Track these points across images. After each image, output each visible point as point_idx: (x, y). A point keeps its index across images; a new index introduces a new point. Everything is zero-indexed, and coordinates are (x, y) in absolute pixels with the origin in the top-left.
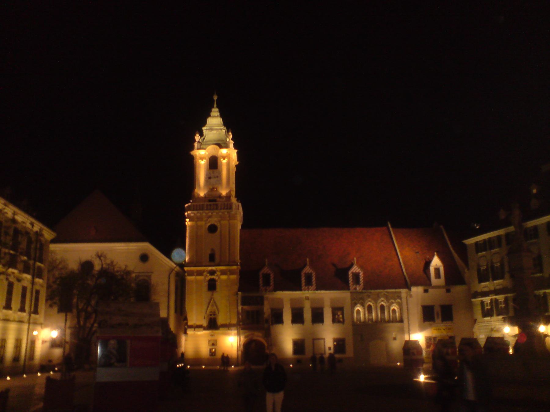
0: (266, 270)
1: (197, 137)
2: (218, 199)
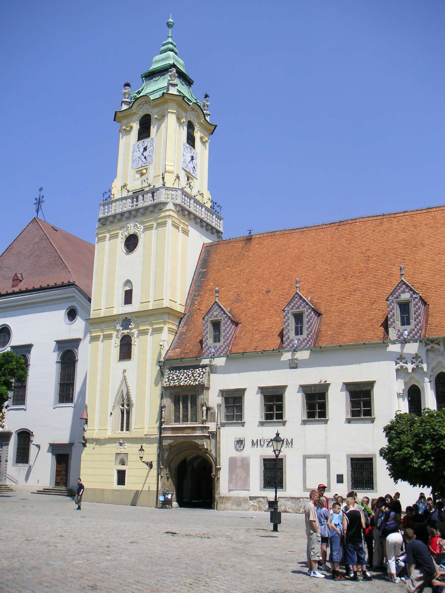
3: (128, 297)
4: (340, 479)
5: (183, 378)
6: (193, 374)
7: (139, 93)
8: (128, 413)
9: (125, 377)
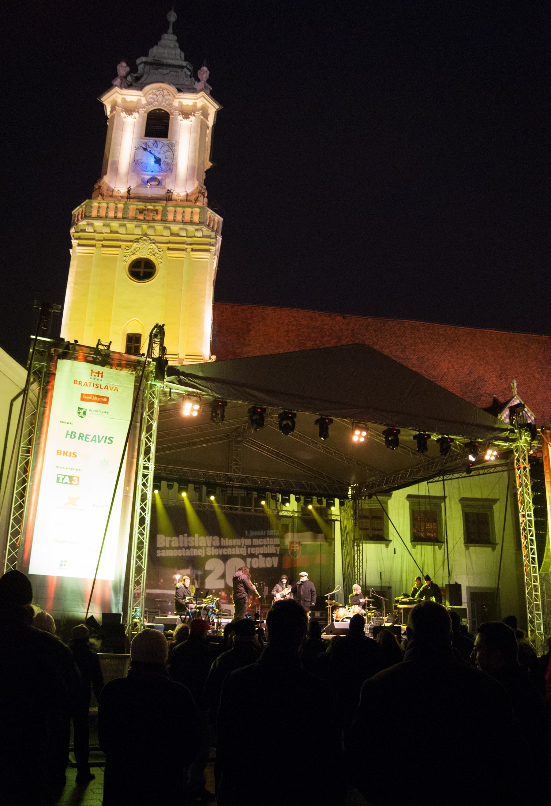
1: (123, 68)
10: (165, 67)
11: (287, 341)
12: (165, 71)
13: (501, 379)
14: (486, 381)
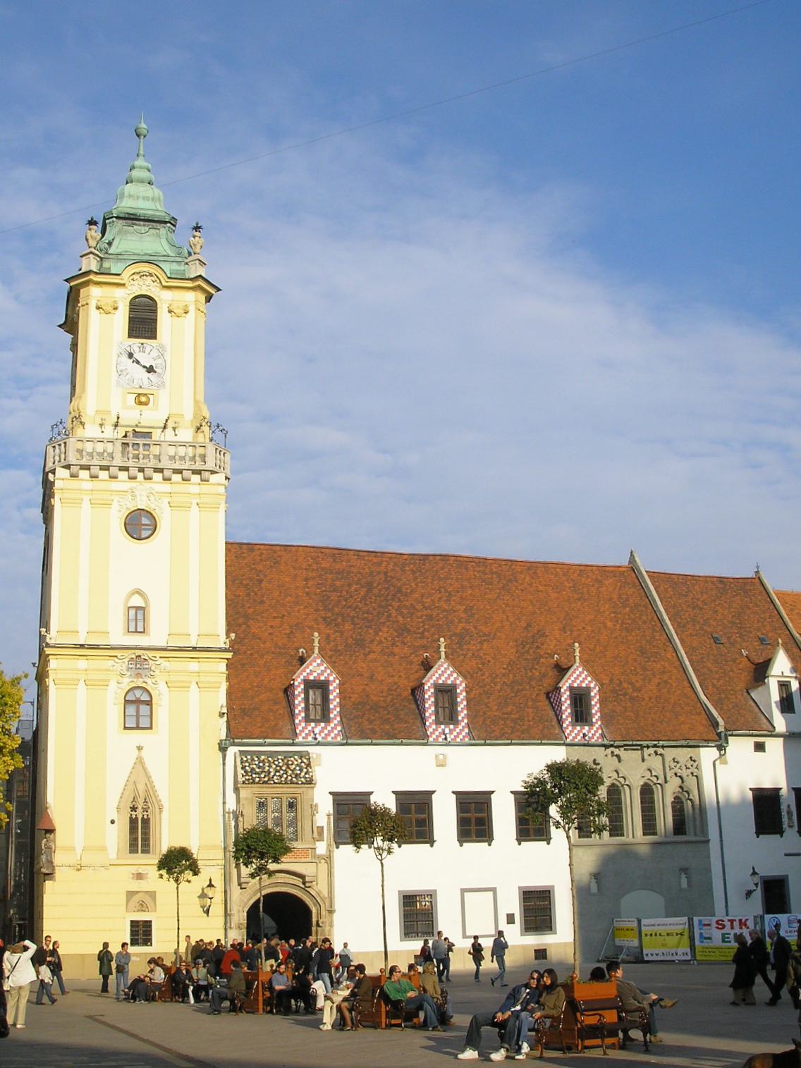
0: (316, 668)
2: (157, 435)
3: (138, 617)
4: (510, 918)
5: (271, 770)
6: (288, 765)
7: (110, 244)
8: (146, 822)
9: (140, 761)
10: (142, 223)
11: (308, 594)
12: (143, 229)
13: (565, 633)
14: (547, 636)
